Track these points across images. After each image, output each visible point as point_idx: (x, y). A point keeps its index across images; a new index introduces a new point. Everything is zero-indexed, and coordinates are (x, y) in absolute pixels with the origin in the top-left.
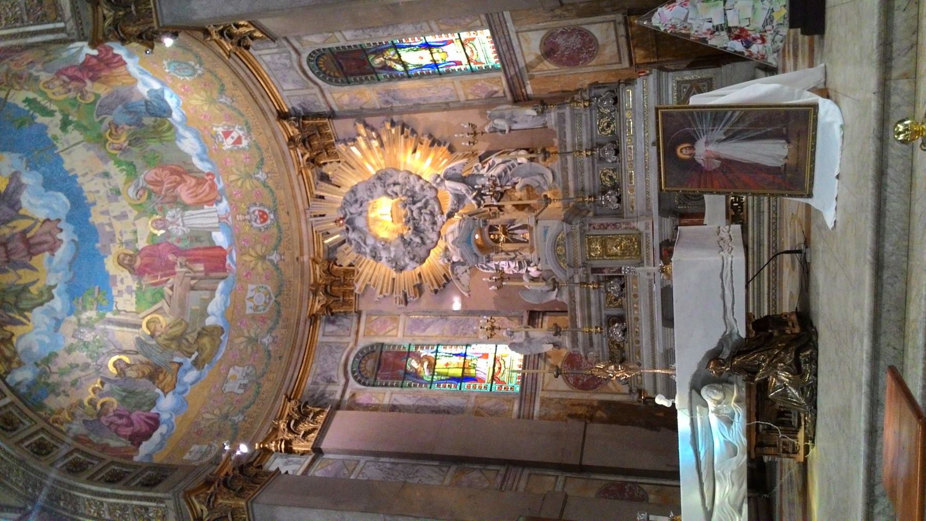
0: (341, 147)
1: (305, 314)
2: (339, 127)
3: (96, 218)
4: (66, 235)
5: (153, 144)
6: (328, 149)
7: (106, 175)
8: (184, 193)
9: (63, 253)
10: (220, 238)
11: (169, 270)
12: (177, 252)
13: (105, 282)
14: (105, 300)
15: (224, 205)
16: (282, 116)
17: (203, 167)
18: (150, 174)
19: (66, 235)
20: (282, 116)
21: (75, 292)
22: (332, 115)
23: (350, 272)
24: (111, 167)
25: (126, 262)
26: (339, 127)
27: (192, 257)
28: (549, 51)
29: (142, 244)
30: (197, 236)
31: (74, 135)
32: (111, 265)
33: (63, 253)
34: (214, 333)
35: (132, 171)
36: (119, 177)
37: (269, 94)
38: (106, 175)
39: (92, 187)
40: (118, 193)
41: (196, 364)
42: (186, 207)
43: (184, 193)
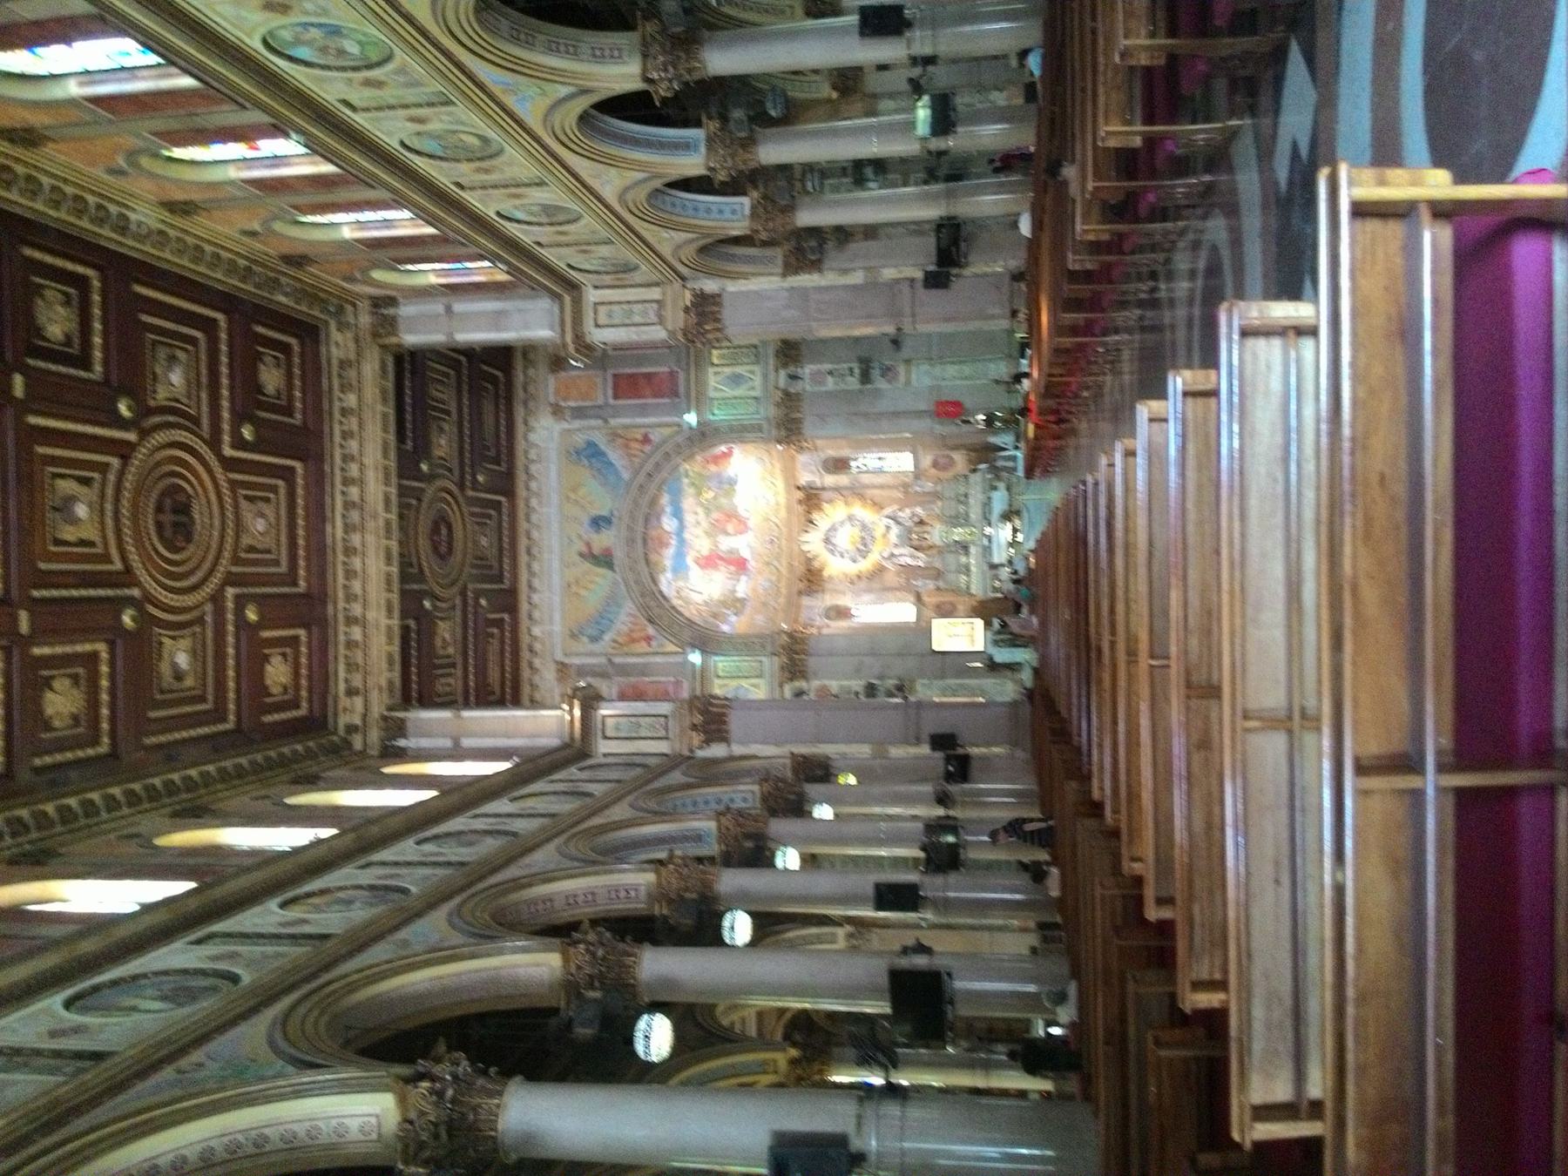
0: (825, 506)
1: (795, 590)
2: (825, 495)
3: (686, 535)
4: (673, 542)
5: (723, 501)
6: (819, 508)
7: (696, 513)
8: (730, 528)
12: (721, 558)
13: (687, 568)
14: (686, 578)
16: (799, 488)
18: (715, 515)
20: (799, 488)
21: (675, 571)
22: (823, 489)
24: (700, 510)
25: (697, 562)
26: (825, 495)
27: (728, 562)
28: (935, 465)
30: (731, 552)
31: (691, 491)
34: (742, 601)
35: (708, 511)
37: (794, 477)
38: (696, 513)
39: (689, 518)
40: (698, 523)
41: (736, 614)
42: (727, 534)
43: (730, 528)
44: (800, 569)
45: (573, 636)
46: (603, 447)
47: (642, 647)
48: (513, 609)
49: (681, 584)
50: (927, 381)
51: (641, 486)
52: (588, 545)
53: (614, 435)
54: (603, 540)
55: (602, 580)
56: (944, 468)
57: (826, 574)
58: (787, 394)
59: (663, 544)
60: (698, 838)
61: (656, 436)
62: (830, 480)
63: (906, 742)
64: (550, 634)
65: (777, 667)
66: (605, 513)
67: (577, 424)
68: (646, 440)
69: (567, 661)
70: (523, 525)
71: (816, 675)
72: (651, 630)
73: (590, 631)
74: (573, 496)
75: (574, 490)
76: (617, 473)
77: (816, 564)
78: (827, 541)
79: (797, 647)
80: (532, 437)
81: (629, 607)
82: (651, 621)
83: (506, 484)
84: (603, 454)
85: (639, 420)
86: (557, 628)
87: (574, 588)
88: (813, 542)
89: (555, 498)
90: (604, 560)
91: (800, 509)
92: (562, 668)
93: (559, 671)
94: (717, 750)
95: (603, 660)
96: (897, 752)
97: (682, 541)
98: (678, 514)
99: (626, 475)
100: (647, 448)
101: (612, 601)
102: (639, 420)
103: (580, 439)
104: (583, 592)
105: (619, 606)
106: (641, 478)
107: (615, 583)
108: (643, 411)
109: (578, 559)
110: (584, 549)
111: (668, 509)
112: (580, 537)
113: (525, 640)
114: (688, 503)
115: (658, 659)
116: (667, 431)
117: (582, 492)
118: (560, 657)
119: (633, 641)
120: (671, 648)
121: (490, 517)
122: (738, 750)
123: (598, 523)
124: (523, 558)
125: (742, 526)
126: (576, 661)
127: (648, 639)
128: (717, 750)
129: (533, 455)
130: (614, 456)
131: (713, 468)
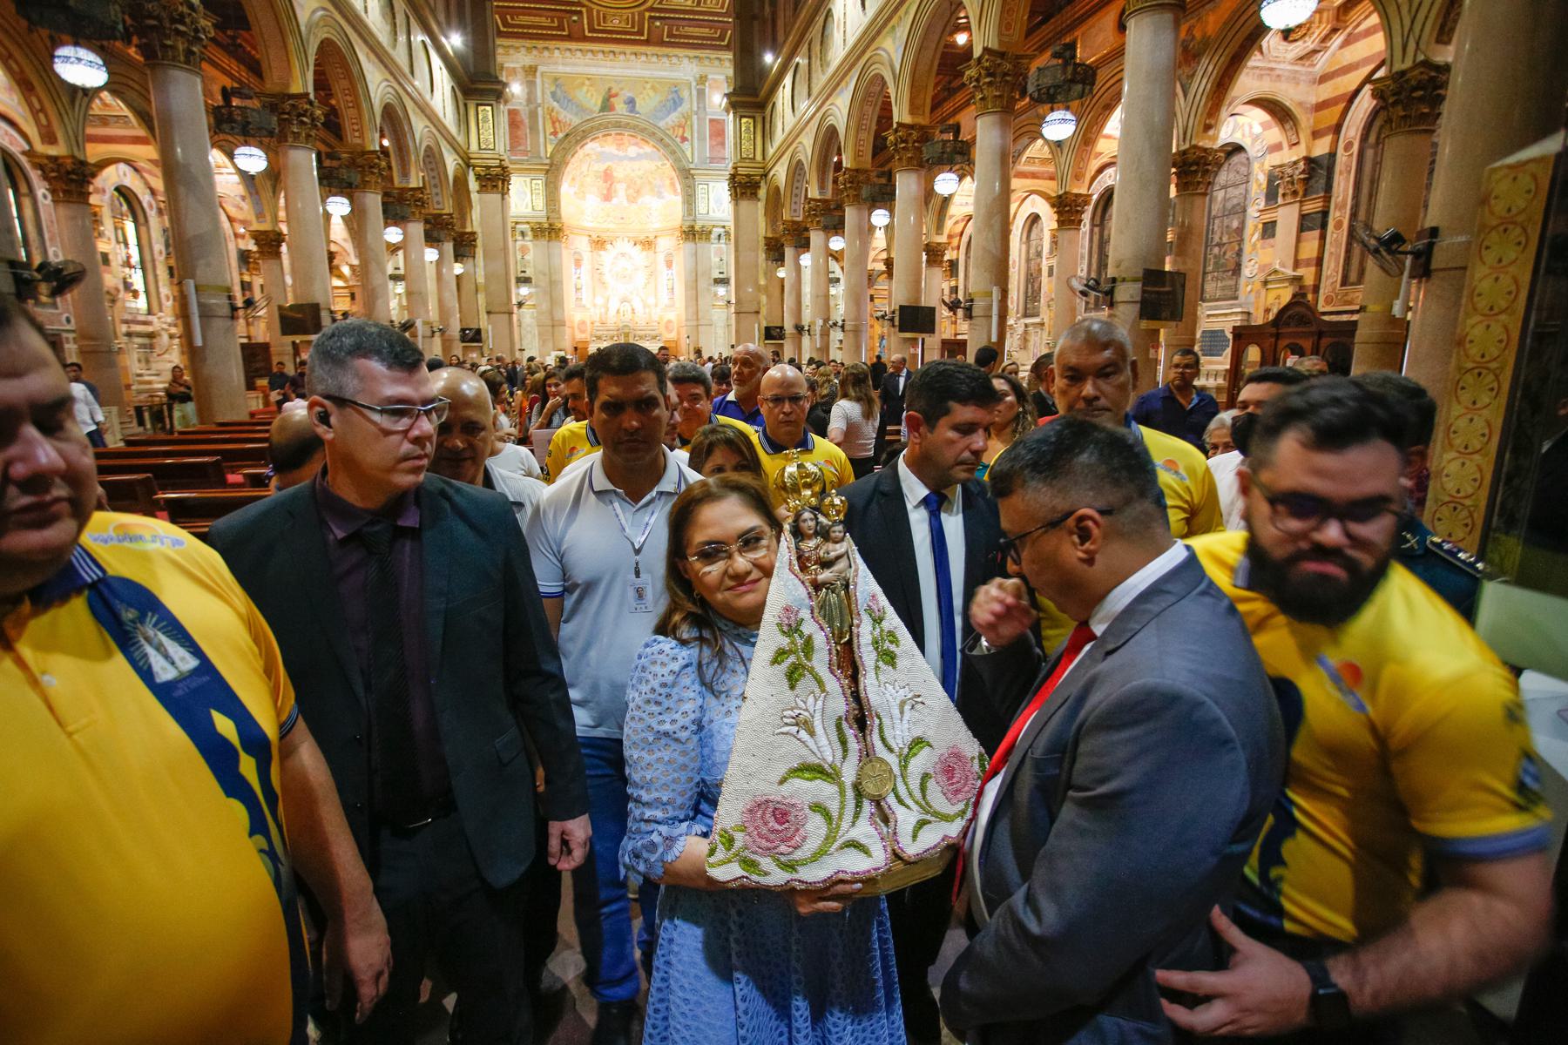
2: (651, 252)
3: (625, 162)
4: (621, 154)
8: (631, 191)
9: (616, 152)
10: (615, 200)
11: (605, 181)
15: (625, 203)
17: (640, 200)
19: (621, 154)
23: (605, 249)
28: (669, 322)
29: (615, 174)
32: (608, 164)
33: (616, 152)
36: (640, 173)
39: (636, 165)
43: (631, 191)
44: (604, 236)
45: (556, 79)
46: (679, 109)
47: (550, 129)
48: (569, 38)
49: (594, 157)
50: (715, 318)
51: (654, 134)
52: (615, 96)
53: (687, 117)
54: (620, 107)
55: (593, 101)
56: (667, 327)
57: (602, 252)
58: (710, 232)
59: (619, 145)
60: (405, 174)
61: (686, 146)
62: (661, 258)
63: (488, 304)
64: (556, 63)
65: (539, 220)
66: (637, 108)
67: (694, 93)
68: (684, 139)
69: (538, 74)
70: (629, 49)
71: (535, 246)
72: (561, 135)
73: (559, 92)
74: (648, 86)
75: (653, 88)
76: (662, 119)
77: (608, 246)
78: (623, 255)
79: (553, 234)
80: (686, 61)
81: (576, 121)
82: (567, 135)
83: (654, 40)
84: (675, 109)
85: (696, 135)
86: (561, 69)
87: (587, 82)
88: (623, 246)
89: (646, 73)
90: (607, 106)
91: (642, 237)
92: (531, 71)
93: (531, 67)
94: (473, 185)
95: (539, 101)
96: (481, 298)
97: (621, 159)
98: (639, 157)
99: (661, 124)
100: (678, 140)
101: (581, 109)
102: (696, 135)
103: (685, 94)
104: (585, 89)
105: (576, 114)
106: (660, 135)
107: (592, 112)
108: (702, 139)
109: (607, 87)
110: (614, 91)
111: (641, 151)
112: (622, 89)
113: (552, 44)
114: (647, 165)
115: (542, 140)
116: (689, 154)
117: (651, 93)
118: (541, 69)
119: (553, 123)
120: (550, 149)
121: (633, 27)
122: (474, 197)
123: (631, 102)
124: (607, 47)
125: (632, 199)
126: (538, 81)
127: (555, 133)
128: (473, 185)
129: (674, 60)
130: (674, 117)
131: (668, 182)
